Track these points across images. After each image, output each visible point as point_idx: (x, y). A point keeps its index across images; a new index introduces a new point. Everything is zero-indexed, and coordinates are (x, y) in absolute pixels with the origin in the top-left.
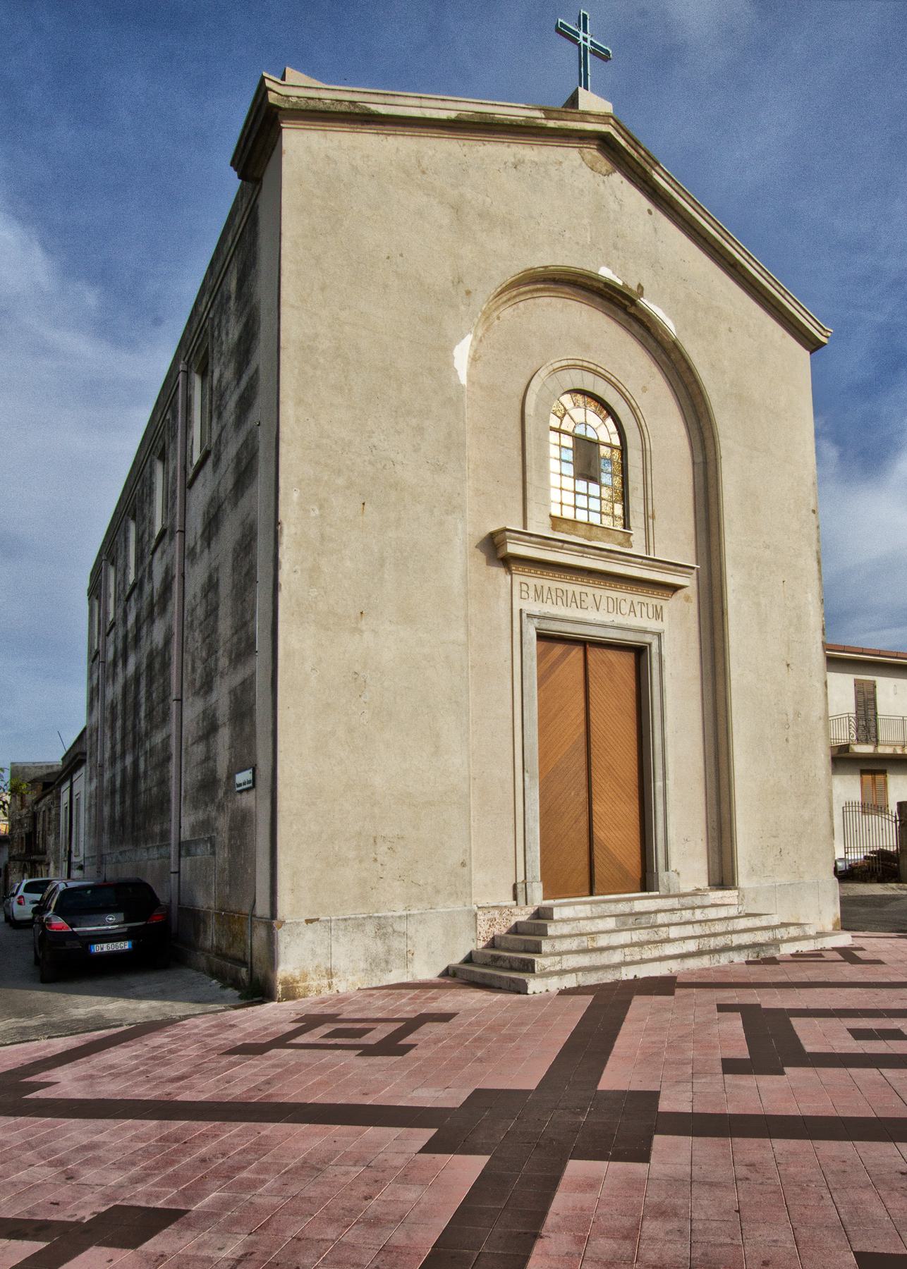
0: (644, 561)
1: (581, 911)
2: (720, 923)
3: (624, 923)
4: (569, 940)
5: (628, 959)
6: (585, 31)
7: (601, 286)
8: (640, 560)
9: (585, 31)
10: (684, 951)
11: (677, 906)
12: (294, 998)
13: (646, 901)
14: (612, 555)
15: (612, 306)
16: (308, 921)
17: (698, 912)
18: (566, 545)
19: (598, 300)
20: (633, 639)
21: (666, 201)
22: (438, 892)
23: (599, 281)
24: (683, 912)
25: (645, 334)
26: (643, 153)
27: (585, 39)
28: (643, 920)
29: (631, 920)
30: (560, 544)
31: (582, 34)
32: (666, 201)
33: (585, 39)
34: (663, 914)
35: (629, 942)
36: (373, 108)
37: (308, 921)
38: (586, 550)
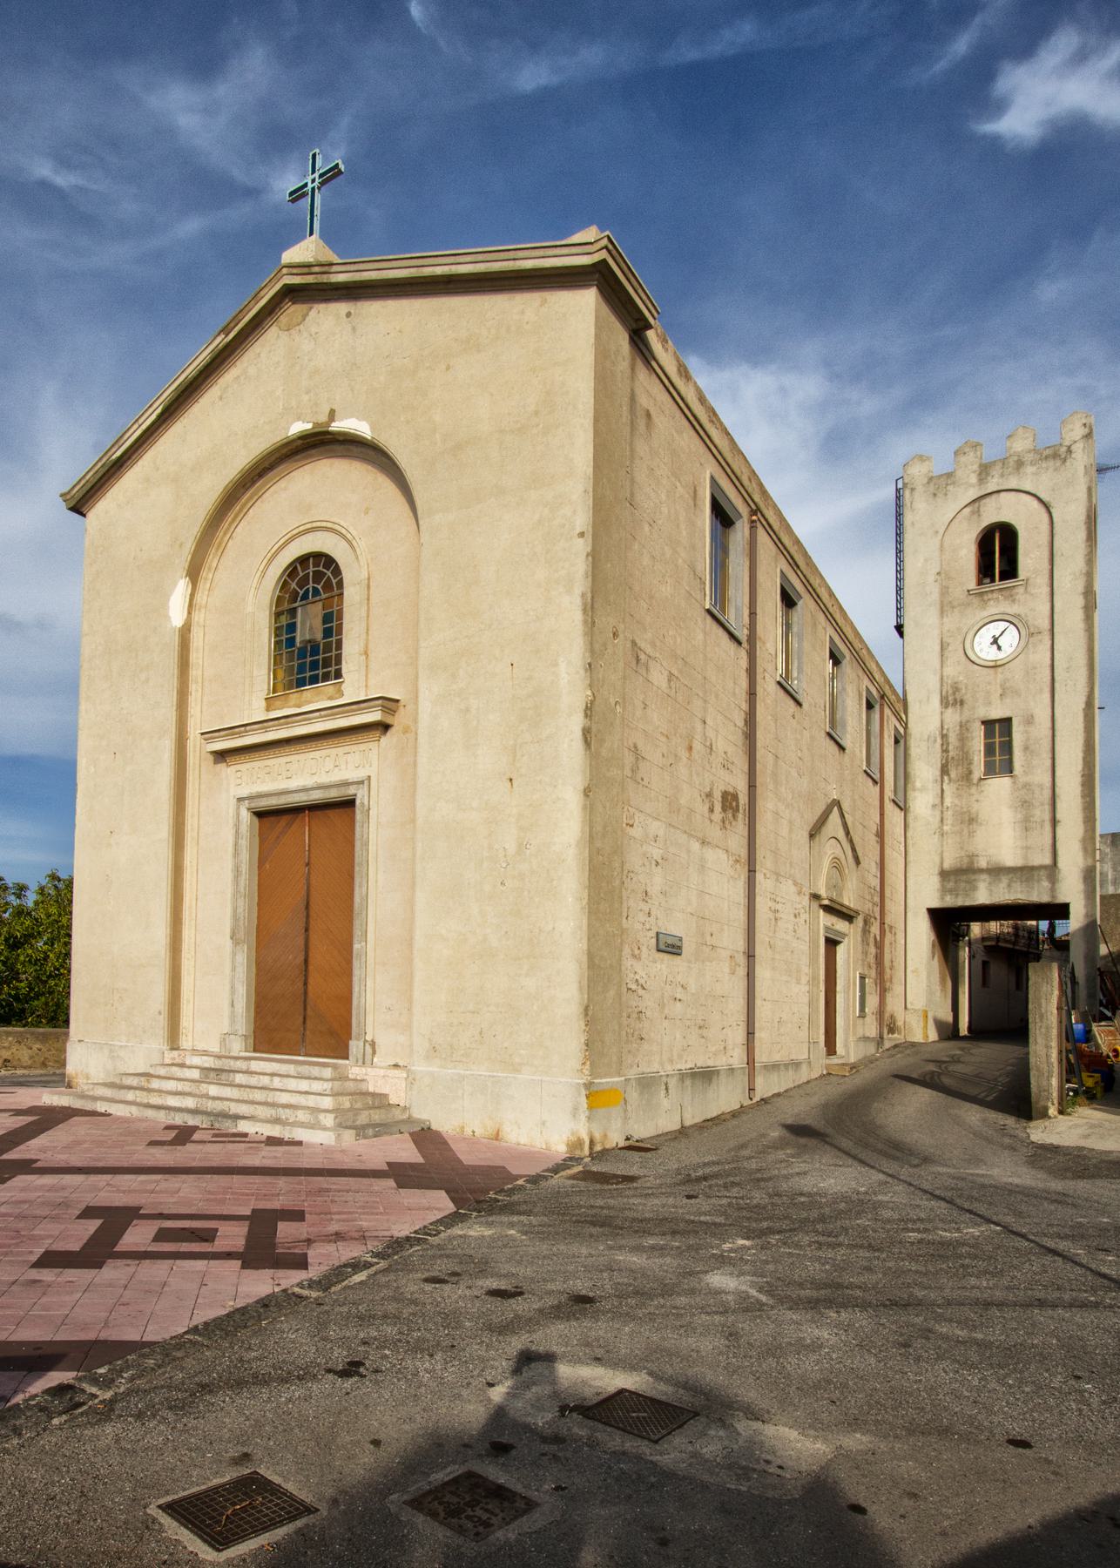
0: (323, 713)
1: (206, 1061)
2: (259, 1091)
3: (207, 1077)
4: (132, 1078)
5: (138, 1100)
6: (306, 185)
7: (300, 442)
8: (317, 714)
9: (306, 185)
10: (183, 1106)
11: (292, 1073)
12: (71, 1087)
13: (262, 1063)
14: (290, 720)
15: (327, 447)
16: (79, 1041)
17: (276, 1079)
18: (248, 728)
19: (314, 451)
20: (336, 795)
21: (360, 287)
22: (144, 1032)
23: (293, 441)
24: (261, 1077)
25: (363, 449)
26: (316, 269)
27: (313, 181)
28: (224, 1076)
29: (212, 1075)
30: (243, 729)
31: (310, 186)
32: (360, 287)
33: (313, 181)
34: (241, 1075)
35: (174, 1090)
36: (114, 457)
37: (79, 1041)
38: (265, 724)
